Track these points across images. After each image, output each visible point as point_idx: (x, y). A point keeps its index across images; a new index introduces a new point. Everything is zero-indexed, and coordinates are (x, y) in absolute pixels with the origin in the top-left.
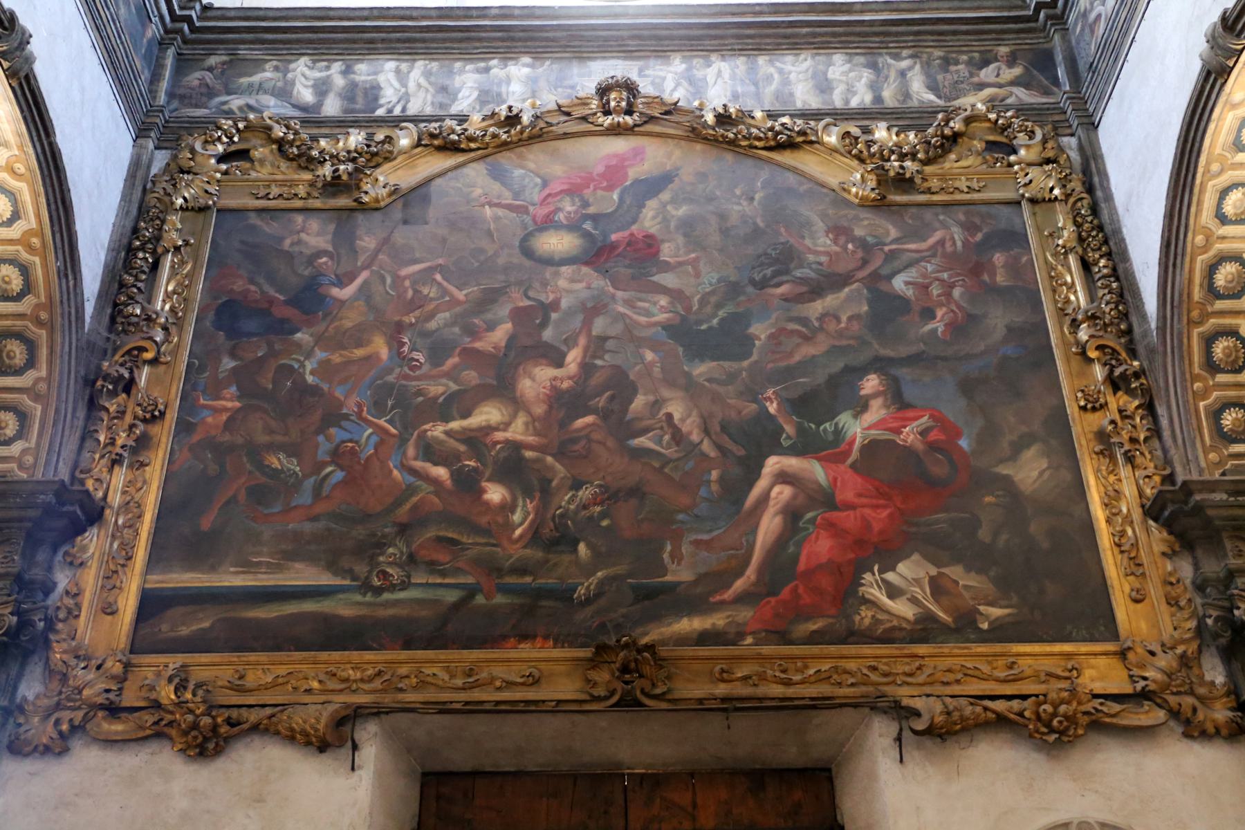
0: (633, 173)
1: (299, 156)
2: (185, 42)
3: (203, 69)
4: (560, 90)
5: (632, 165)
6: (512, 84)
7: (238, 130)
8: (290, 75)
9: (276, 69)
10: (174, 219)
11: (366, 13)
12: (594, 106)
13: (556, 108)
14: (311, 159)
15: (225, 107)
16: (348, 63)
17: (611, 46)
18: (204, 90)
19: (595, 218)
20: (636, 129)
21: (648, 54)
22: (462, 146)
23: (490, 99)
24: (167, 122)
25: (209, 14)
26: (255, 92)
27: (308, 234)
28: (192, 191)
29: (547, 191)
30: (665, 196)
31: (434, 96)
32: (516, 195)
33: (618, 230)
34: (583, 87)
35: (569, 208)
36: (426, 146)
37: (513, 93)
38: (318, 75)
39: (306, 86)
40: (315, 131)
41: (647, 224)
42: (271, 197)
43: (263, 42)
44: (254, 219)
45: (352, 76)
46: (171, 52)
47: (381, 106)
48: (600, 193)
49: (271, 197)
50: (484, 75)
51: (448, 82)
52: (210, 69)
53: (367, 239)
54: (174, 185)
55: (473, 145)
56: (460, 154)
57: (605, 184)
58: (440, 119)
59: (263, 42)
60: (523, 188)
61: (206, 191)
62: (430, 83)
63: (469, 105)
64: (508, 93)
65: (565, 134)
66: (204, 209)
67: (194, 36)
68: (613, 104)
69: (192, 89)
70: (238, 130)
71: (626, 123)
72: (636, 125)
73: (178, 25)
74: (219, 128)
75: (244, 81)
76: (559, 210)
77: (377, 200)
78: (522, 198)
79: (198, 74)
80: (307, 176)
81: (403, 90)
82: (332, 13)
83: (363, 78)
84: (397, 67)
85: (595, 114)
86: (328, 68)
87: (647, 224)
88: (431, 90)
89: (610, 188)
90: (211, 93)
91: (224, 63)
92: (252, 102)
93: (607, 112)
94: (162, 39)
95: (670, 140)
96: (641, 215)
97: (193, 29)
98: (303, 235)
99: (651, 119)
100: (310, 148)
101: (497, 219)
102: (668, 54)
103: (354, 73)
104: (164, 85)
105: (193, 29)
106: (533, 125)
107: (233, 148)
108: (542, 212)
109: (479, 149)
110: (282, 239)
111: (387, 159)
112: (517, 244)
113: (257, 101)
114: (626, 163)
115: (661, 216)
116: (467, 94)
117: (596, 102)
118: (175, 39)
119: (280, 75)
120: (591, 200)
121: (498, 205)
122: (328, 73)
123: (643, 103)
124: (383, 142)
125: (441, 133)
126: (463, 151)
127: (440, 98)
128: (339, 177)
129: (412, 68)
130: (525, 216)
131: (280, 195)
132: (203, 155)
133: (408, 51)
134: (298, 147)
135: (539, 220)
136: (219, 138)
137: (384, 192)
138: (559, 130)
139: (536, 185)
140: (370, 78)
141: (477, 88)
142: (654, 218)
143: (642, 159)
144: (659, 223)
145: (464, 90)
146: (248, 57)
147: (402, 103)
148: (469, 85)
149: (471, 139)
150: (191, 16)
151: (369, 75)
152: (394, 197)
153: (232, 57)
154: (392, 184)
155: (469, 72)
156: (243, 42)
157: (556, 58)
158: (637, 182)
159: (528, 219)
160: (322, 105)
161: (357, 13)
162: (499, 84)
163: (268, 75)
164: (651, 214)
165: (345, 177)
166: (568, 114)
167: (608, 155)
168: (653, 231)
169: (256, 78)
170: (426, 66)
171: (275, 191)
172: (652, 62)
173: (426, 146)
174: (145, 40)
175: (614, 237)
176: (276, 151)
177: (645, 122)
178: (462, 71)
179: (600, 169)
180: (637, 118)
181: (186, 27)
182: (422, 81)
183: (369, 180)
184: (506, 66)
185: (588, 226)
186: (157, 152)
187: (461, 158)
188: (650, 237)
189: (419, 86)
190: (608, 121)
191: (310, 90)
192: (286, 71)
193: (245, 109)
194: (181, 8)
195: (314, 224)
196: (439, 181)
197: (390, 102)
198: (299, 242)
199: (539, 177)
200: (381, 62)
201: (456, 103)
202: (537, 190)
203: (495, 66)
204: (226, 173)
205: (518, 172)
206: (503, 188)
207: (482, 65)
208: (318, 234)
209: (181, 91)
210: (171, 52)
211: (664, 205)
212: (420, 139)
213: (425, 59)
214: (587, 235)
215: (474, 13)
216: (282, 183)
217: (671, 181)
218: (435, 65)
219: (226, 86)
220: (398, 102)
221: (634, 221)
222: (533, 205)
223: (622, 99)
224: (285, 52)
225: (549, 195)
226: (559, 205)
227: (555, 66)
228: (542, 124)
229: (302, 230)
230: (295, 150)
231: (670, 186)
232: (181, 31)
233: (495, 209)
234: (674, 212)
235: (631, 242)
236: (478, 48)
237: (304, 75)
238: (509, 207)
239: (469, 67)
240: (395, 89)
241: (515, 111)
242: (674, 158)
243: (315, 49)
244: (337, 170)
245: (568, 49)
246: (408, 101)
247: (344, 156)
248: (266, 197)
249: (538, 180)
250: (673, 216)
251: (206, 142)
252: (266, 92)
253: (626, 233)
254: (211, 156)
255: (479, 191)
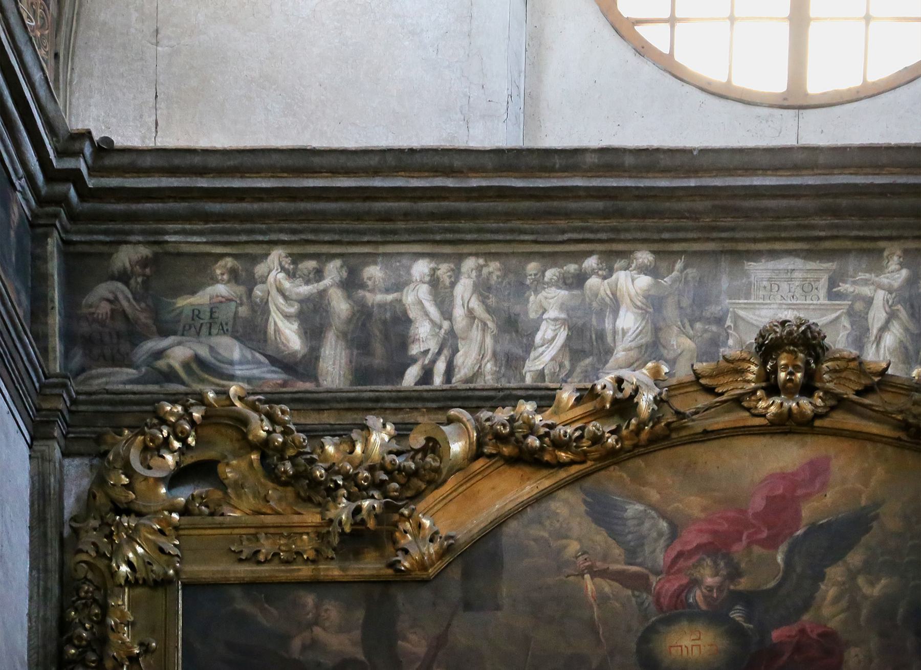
0: (810, 511)
1: (297, 476)
2: (74, 217)
3: (113, 278)
4: (698, 326)
5: (807, 496)
6: (622, 313)
7: (192, 423)
8: (258, 291)
9: (234, 277)
10: (122, 601)
11: (374, 161)
12: (751, 377)
13: (693, 378)
14: (315, 483)
15: (161, 364)
16: (353, 261)
17: (785, 228)
18: (120, 325)
19: (747, 599)
20: (818, 423)
21: (848, 244)
22: (547, 457)
23: (587, 347)
24: (74, 402)
25: (108, 161)
26: (205, 330)
27: (324, 629)
28: (140, 550)
29: (677, 547)
30: (855, 558)
31: (496, 339)
32: (632, 555)
33: (785, 621)
34: (737, 318)
35: (710, 581)
36: (490, 456)
37: (624, 333)
38: (305, 290)
39: (287, 317)
40: (312, 419)
41: (827, 611)
42: (261, 558)
43: (207, 217)
44: (242, 604)
45: (361, 293)
46: (52, 245)
47: (414, 360)
48: (757, 550)
49: (261, 558)
50: (575, 292)
51: (517, 309)
52: (124, 277)
53: (413, 637)
54: (110, 536)
55: (563, 456)
56: (545, 472)
57: (765, 534)
58: (508, 398)
59: (207, 217)
60: (641, 540)
61: (162, 550)
62: (489, 310)
63: (553, 359)
64: (615, 332)
65: (705, 432)
66: (164, 583)
67: (87, 206)
68: (782, 375)
69: (102, 323)
70: (192, 423)
71: (802, 413)
72: (817, 416)
73: (59, 188)
74: (163, 421)
75: (184, 302)
76: (695, 582)
77: (423, 566)
78: (639, 560)
79: (104, 289)
80: (312, 517)
81: (446, 325)
82: (317, 161)
83: (379, 298)
84: (434, 270)
85: (753, 392)
86: (319, 274)
87: (827, 611)
88: (490, 324)
89: (771, 543)
90: (135, 336)
91: (145, 262)
92: (204, 352)
93: (772, 389)
94: (35, 215)
95: (869, 446)
96: (818, 595)
97: (85, 194)
98: (317, 630)
99: (839, 403)
100: (312, 462)
101: (603, 599)
102: (882, 244)
103: (363, 286)
104: (55, 320)
105: (85, 194)
106: (654, 417)
107: (189, 460)
108: (672, 586)
109: (572, 463)
110: (285, 639)
111: (435, 483)
112: (633, 646)
113: (211, 349)
114: (799, 492)
115: (847, 597)
116: (549, 334)
117: (754, 368)
118: (56, 216)
119: (241, 290)
120: (743, 565)
121: (604, 574)
122: (322, 285)
123: (833, 371)
124: (424, 450)
125: (512, 433)
126: (548, 465)
127: (507, 345)
128: (363, 522)
129: (456, 275)
130: (645, 595)
131: (276, 555)
132: (146, 478)
133: (449, 236)
134: (291, 459)
135: (665, 601)
136: (166, 443)
137: (433, 549)
138: (698, 425)
139: (660, 534)
140: (390, 297)
141: (564, 322)
142: (837, 600)
143: (824, 485)
144: (843, 611)
145: (543, 326)
146: (186, 248)
147: (446, 352)
148: (552, 313)
149: (560, 444)
150: (79, 171)
151: (387, 291)
152: (448, 559)
153: (157, 249)
154: (443, 533)
155: (550, 284)
156: (173, 217)
157: (695, 253)
158: (814, 529)
159: (649, 600)
160: (317, 358)
161: (362, 162)
162: (601, 314)
163: (222, 289)
164: (832, 592)
165: (371, 524)
166: (710, 390)
167: (772, 476)
168: (833, 624)
169: (202, 298)
170: (479, 269)
171: (266, 547)
172: (852, 263)
173: (490, 456)
174: (12, 233)
175: (776, 635)
176: (256, 464)
177: (833, 408)
178: (539, 284)
179: (758, 503)
180: (819, 402)
181: (72, 192)
182: (475, 304)
183: (408, 526)
184: (611, 271)
185: (737, 615)
186: (67, 462)
187: (543, 482)
188: (828, 635)
189: (471, 315)
190: (771, 406)
191: (295, 326)
192: (250, 282)
193: (194, 366)
194: (60, 154)
195: (333, 611)
196: (513, 526)
197: (426, 352)
198: (313, 645)
199: (664, 517)
200: (405, 261)
201: (533, 354)
202: (662, 543)
203: (593, 272)
204: (185, 511)
205: (634, 509)
206: (610, 540)
207: (572, 268)
208: (341, 630)
209: (84, 328)
210: (52, 245)
211: (852, 575)
212: (480, 443)
213: (477, 255)
214: (735, 632)
215: (558, 161)
216: (275, 531)
217: (868, 530)
218: (494, 266)
219: (155, 312)
220: (439, 353)
221: (807, 605)
222: (657, 573)
223: (797, 368)
224: (244, 238)
225: (680, 555)
226: (697, 575)
227: (692, 272)
228: (670, 417)
229: (316, 622)
230: (289, 467)
231: (864, 540)
232: (63, 200)
233: (598, 580)
234: (867, 590)
235: (800, 645)
236: (563, 232)
237: (281, 291)
238: (620, 577)
239: (551, 274)
240: (431, 320)
241: (628, 389)
242: (873, 482)
243: (294, 232)
244: (358, 510)
245: (715, 235)
246: (455, 351)
247: (366, 479)
248: (253, 559)
249: (664, 525)
250: (865, 597)
251: (145, 449)
252: (225, 332)
253: (793, 629)
254: (158, 480)
255: (574, 547)
